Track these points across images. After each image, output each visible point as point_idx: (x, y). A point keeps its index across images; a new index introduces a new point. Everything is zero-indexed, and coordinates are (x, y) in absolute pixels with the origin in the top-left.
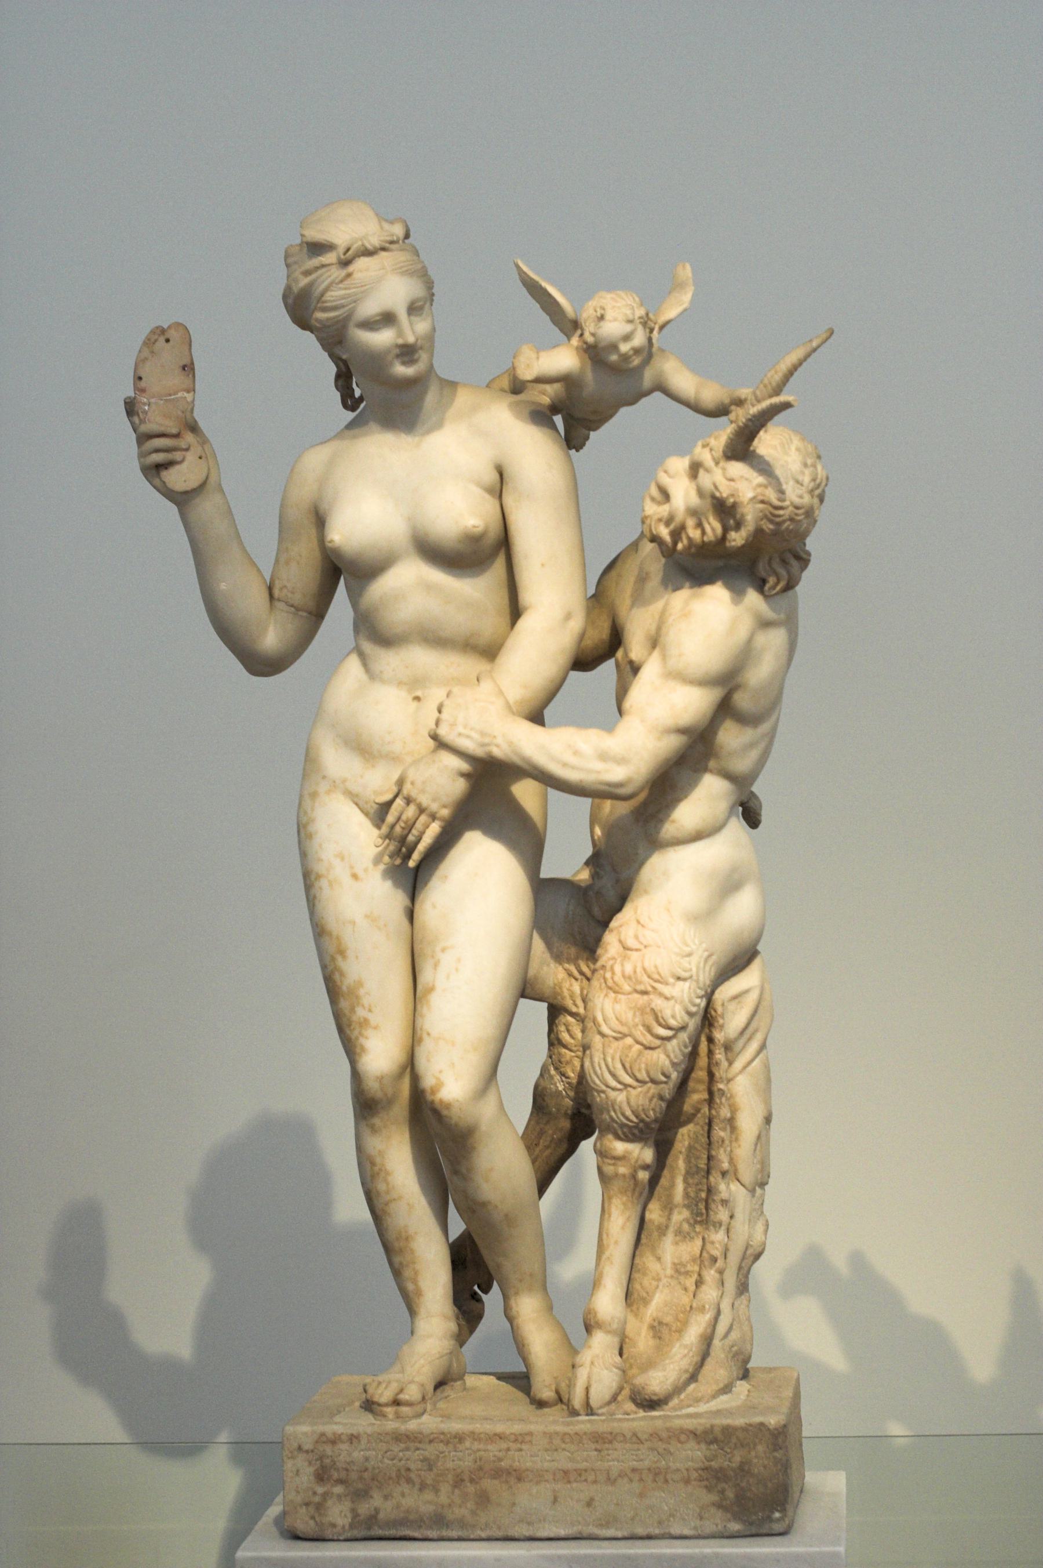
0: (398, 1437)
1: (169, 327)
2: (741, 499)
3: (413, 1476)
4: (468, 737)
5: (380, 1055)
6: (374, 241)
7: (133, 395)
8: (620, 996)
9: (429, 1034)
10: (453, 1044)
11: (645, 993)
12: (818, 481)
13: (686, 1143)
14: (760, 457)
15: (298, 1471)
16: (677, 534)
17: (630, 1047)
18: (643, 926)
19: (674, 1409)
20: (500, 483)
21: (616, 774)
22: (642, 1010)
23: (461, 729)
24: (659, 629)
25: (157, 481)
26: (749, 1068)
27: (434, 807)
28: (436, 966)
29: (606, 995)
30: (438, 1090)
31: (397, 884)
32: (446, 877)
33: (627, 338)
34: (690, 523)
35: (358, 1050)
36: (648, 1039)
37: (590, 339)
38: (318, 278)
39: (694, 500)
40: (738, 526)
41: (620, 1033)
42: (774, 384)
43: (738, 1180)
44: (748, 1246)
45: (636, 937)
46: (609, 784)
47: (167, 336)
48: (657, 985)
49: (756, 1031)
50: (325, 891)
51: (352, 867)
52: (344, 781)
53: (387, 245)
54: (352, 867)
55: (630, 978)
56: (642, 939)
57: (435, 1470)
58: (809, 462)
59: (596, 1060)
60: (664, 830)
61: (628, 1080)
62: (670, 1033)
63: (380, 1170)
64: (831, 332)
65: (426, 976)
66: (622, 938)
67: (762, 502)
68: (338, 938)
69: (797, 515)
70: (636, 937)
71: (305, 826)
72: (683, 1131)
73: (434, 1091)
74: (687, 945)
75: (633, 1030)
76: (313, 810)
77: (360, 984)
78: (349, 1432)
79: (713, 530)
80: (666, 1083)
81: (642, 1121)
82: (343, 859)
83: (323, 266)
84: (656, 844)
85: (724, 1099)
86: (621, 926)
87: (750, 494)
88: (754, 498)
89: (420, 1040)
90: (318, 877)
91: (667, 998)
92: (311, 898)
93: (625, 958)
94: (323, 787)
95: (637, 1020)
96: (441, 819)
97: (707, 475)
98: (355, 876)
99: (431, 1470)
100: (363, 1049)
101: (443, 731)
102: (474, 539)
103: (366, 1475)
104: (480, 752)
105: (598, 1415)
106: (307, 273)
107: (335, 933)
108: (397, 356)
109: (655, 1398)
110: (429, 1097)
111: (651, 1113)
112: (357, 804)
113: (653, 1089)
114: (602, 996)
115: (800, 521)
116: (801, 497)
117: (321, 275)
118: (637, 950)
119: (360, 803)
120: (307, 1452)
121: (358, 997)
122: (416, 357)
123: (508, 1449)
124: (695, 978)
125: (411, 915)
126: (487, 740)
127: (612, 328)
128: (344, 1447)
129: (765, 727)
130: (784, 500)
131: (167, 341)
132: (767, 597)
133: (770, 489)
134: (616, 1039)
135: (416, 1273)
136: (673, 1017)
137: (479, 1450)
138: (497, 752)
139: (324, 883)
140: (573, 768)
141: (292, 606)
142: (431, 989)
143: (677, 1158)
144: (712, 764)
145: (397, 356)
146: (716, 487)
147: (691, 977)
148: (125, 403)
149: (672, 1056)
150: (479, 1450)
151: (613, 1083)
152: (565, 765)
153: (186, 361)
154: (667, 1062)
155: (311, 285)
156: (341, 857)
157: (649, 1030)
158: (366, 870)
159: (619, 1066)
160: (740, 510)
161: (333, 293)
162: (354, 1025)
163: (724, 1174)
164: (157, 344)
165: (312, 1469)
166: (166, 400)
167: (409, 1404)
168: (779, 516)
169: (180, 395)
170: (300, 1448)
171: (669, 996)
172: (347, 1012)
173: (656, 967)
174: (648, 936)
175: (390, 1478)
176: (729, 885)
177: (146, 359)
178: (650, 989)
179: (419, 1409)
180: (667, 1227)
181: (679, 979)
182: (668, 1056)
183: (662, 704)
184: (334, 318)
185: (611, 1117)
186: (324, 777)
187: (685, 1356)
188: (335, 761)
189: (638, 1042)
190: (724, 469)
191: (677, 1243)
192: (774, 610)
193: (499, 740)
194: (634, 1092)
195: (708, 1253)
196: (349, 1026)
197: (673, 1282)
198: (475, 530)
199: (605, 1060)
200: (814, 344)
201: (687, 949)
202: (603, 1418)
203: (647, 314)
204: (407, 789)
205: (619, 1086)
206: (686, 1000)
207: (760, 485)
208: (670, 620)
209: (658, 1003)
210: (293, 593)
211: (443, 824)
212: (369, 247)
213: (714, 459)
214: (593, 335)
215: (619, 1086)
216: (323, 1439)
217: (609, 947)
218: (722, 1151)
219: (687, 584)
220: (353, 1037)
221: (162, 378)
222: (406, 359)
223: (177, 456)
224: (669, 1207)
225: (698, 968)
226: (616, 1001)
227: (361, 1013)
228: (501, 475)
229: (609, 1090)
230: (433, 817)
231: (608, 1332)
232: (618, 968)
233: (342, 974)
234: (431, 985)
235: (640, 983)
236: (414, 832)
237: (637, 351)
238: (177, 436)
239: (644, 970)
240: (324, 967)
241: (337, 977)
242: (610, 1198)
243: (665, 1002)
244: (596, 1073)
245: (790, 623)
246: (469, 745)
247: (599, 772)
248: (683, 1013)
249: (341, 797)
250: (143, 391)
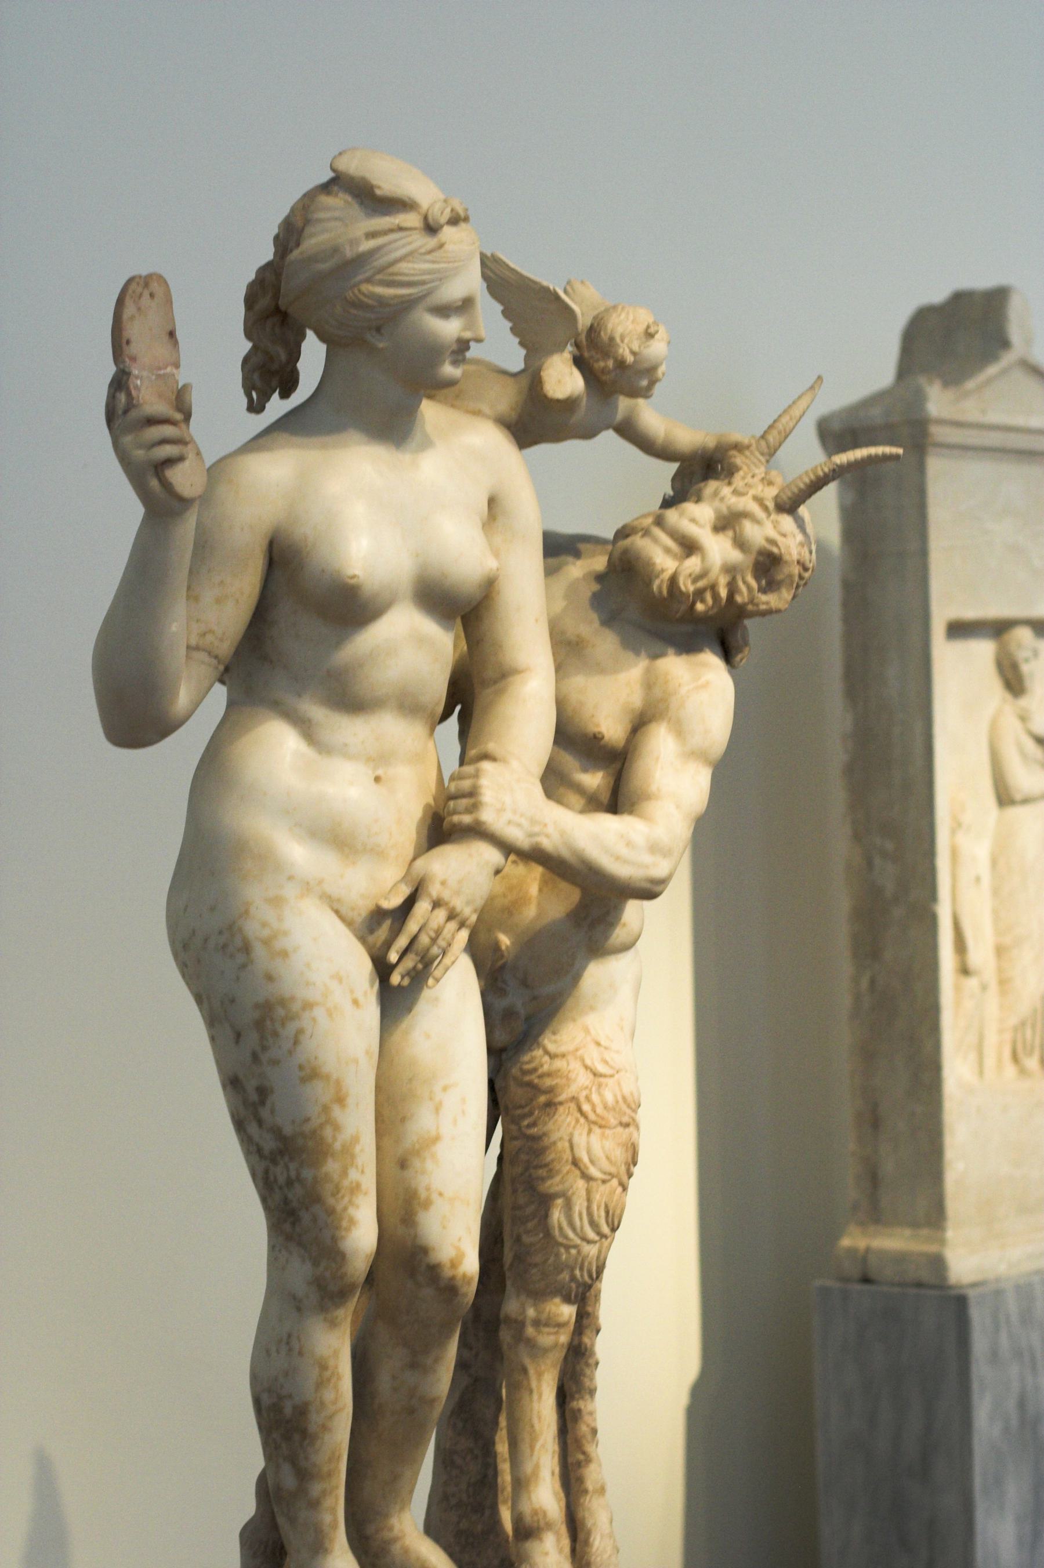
1: (150, 276)
4: (519, 825)
8: (608, 1132)
9: (441, 1194)
10: (468, 1204)
16: (699, 594)
18: (606, 1048)
23: (508, 815)
25: (154, 483)
28: (437, 1110)
29: (590, 1131)
30: (460, 1263)
32: (437, 999)
34: (723, 581)
35: (344, 1224)
37: (630, 359)
38: (390, 243)
39: (735, 556)
40: (771, 586)
41: (610, 1174)
45: (606, 1062)
51: (352, 991)
52: (321, 882)
54: (352, 991)
55: (614, 1109)
56: (611, 1062)
60: (614, 935)
63: (333, 1373)
64: (820, 378)
66: (588, 1062)
67: (798, 562)
68: (338, 1082)
70: (606, 1062)
73: (454, 1264)
76: (280, 919)
77: (355, 1139)
79: (749, 588)
82: (340, 980)
83: (401, 229)
86: (577, 1050)
89: (427, 1204)
90: (308, 1006)
93: (600, 1085)
94: (290, 891)
97: (756, 527)
98: (356, 1002)
100: (352, 1222)
101: (488, 816)
106: (372, 235)
107: (335, 1076)
110: (447, 1273)
112: (337, 912)
114: (585, 1132)
117: (395, 241)
118: (612, 1076)
119: (344, 910)
121: (353, 1157)
126: (536, 829)
131: (152, 295)
134: (604, 1182)
138: (547, 844)
139: (319, 1013)
140: (626, 862)
141: (216, 657)
142: (437, 1139)
145: (453, 352)
146: (773, 542)
151: (591, 1235)
152: (618, 858)
153: (170, 328)
155: (372, 253)
156: (339, 978)
159: (603, 1214)
160: (786, 570)
161: (410, 265)
162: (343, 1191)
166: (159, 376)
172: (336, 1177)
173: (632, 1094)
184: (403, 296)
185: (573, 1278)
186: (291, 878)
188: (298, 853)
193: (550, 830)
195: (588, 1426)
196: (333, 1195)
199: (589, 1208)
204: (435, 890)
205: (597, 1238)
208: (684, 690)
210: (221, 640)
213: (766, 509)
214: (634, 353)
217: (572, 1076)
219: (671, 651)
220: (339, 1208)
227: (353, 1175)
229: (584, 1244)
232: (595, 1097)
233: (337, 1128)
234: (433, 1133)
236: (442, 942)
239: (624, 1099)
241: (328, 1132)
242: (540, 1375)
244: (571, 1224)
246: (517, 835)
247: (647, 867)
250: (133, 359)
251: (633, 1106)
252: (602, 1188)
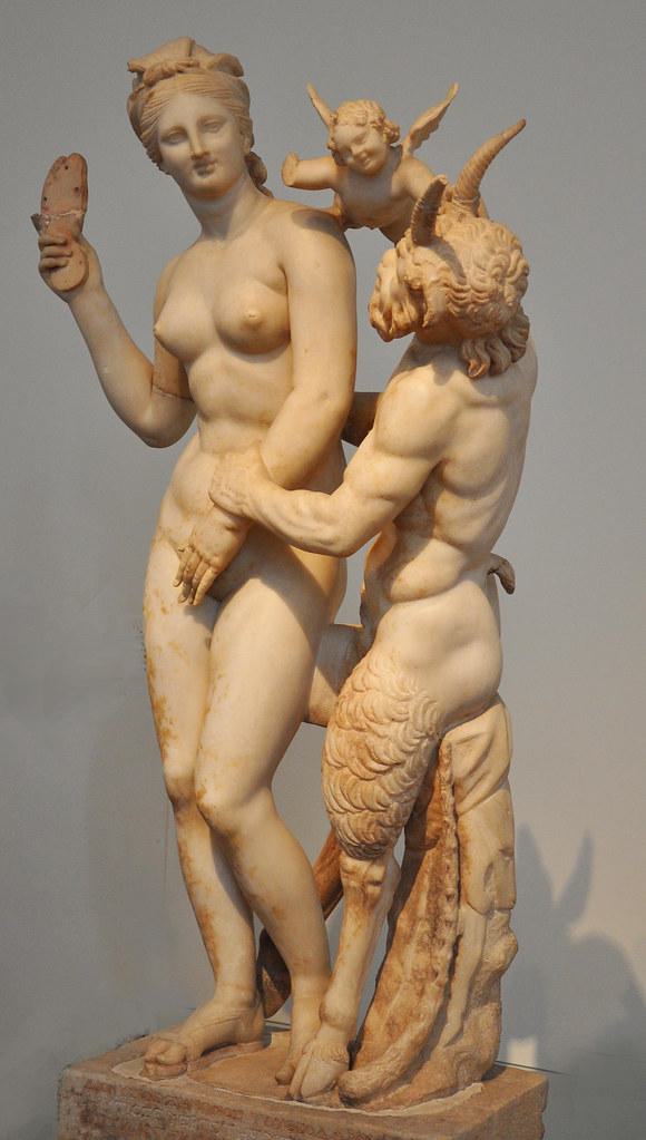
0: (145, 1095)
2: (425, 282)
3: (150, 1131)
4: (228, 496)
5: (176, 762)
6: (172, 65)
8: (343, 731)
11: (361, 730)
12: (510, 269)
13: (431, 864)
14: (447, 243)
15: (69, 1110)
17: (347, 777)
19: (373, 1109)
20: (283, 283)
21: (326, 533)
22: (358, 745)
26: (481, 806)
27: (208, 555)
31: (198, 619)
33: (359, 140)
36: (363, 771)
42: (469, 175)
43: (469, 904)
44: (480, 963)
46: (321, 541)
47: (67, 164)
48: (368, 722)
49: (487, 772)
53: (182, 68)
54: (163, 602)
55: (350, 715)
56: (366, 682)
57: (167, 1131)
58: (497, 249)
61: (348, 806)
62: (384, 768)
64: (524, 121)
67: (446, 285)
69: (478, 298)
70: (363, 679)
72: (429, 853)
73: (200, 797)
74: (403, 690)
75: (349, 761)
78: (109, 1082)
81: (363, 842)
84: (392, 601)
85: (449, 831)
87: (433, 278)
88: (438, 281)
91: (379, 736)
94: (159, 535)
95: (353, 753)
96: (217, 567)
98: (164, 610)
99: (164, 1129)
102: (254, 327)
103: (118, 1124)
104: (235, 510)
105: (307, 1103)
108: (196, 167)
109: (352, 1096)
111: (372, 836)
113: (371, 816)
115: (483, 305)
118: (362, 691)
120: (77, 1094)
122: (210, 167)
123: (223, 1123)
124: (411, 720)
125: (209, 643)
126: (239, 499)
127: (346, 132)
128: (103, 1095)
129: (488, 500)
130: (464, 284)
131: (67, 168)
132: (474, 379)
133: (452, 273)
135: (215, 946)
136: (386, 753)
137: (202, 1119)
140: (295, 525)
143: (423, 876)
144: (436, 531)
145: (196, 167)
147: (407, 719)
148: (32, 218)
149: (387, 787)
150: (202, 1119)
151: (336, 807)
152: (290, 523)
153: (78, 184)
154: (383, 793)
157: (363, 762)
163: (449, 897)
164: (60, 171)
165: (78, 1111)
167: (166, 1065)
168: (462, 299)
169: (72, 212)
170: (73, 1090)
171: (381, 734)
173: (372, 707)
174: (372, 680)
175: (134, 1129)
176: (453, 639)
177: (50, 184)
178: (364, 726)
179: (174, 1069)
180: (411, 936)
181: (393, 720)
182: (384, 788)
183: (375, 470)
187: (393, 1059)
188: (170, 517)
189: (354, 773)
190: (413, 254)
191: (418, 952)
192: (483, 393)
193: (248, 500)
194: (353, 817)
197: (412, 986)
200: (505, 136)
201: (404, 694)
202: (310, 1106)
203: (382, 120)
205: (342, 811)
206: (400, 739)
207: (442, 269)
209: (372, 740)
211: (215, 570)
212: (166, 69)
215: (342, 811)
216: (89, 1085)
218: (447, 876)
221: (65, 202)
222: (202, 169)
223: (62, 261)
224: (414, 920)
225: (415, 712)
226: (339, 735)
228: (284, 271)
230: (208, 563)
231: (333, 1026)
235: (357, 720)
237: (371, 154)
238: (65, 244)
239: (363, 709)
243: (379, 740)
245: (517, 410)
247: (314, 531)
248: (397, 751)
249: (167, 543)
251: (371, 716)
252: (336, 772)
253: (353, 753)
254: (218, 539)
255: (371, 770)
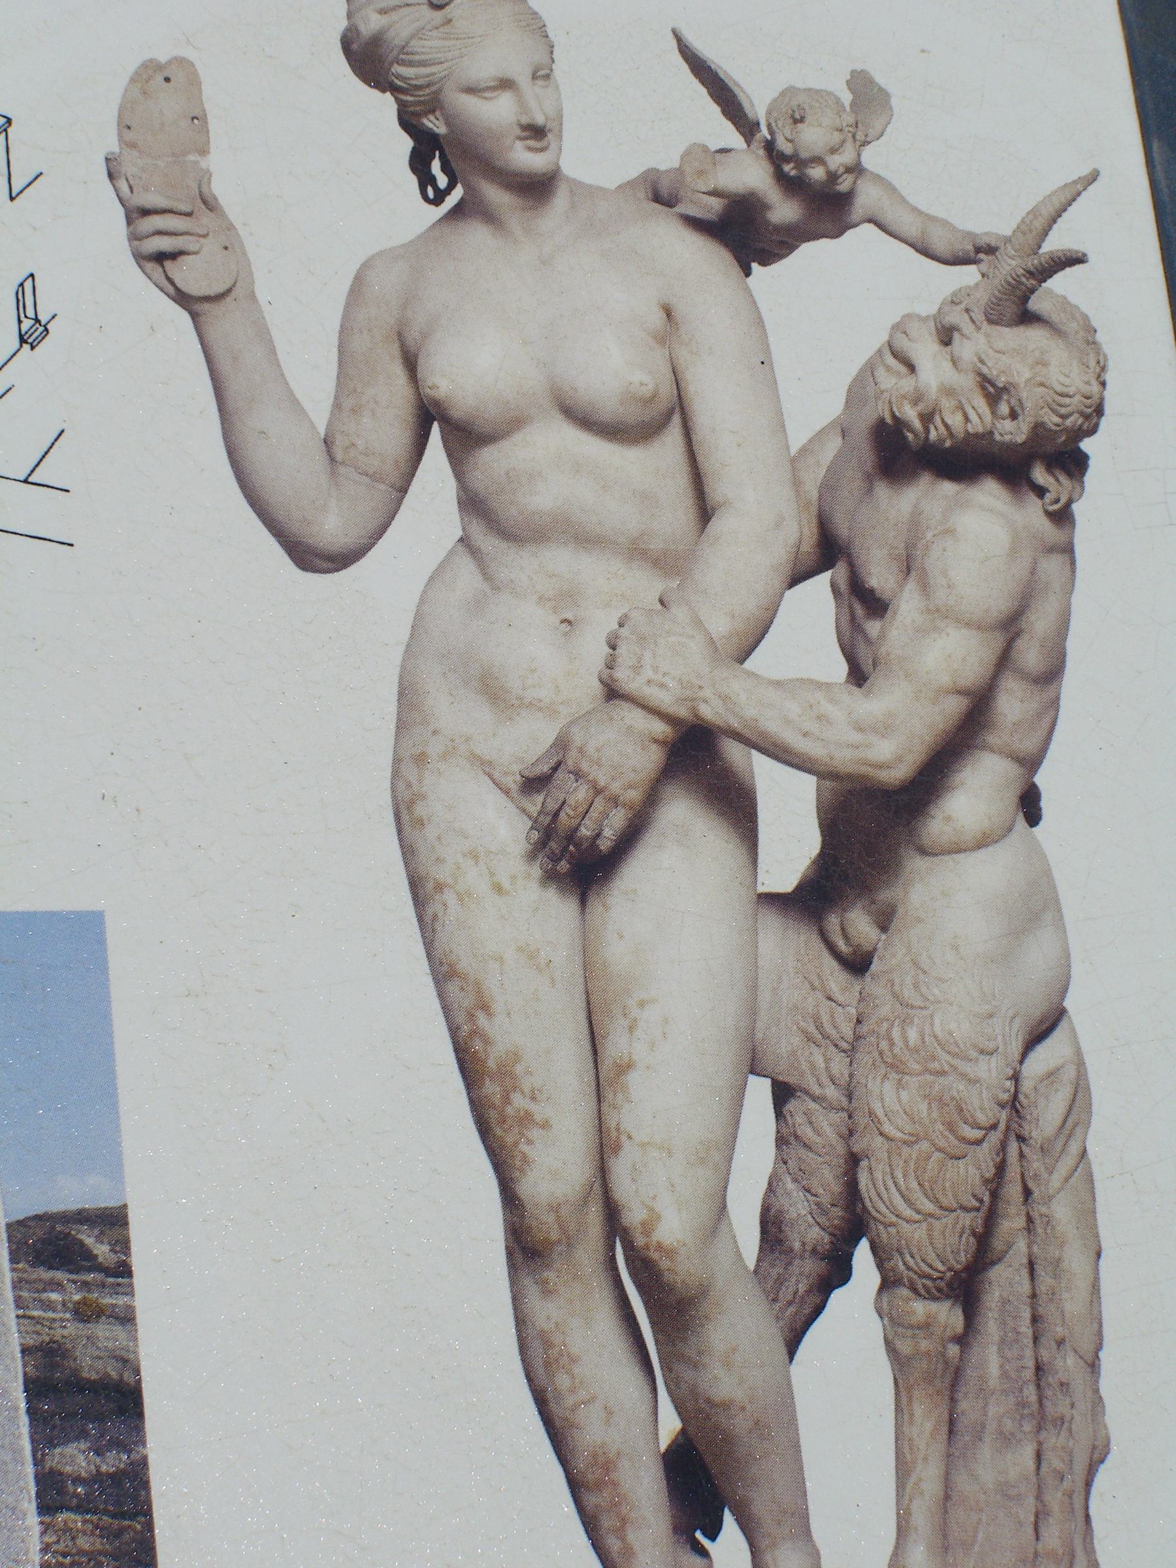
7: (117, 150)
11: (942, 1073)
24: (910, 547)
50: (449, 907)
51: (492, 874)
55: (917, 1051)
59: (878, 1175)
61: (929, 1207)
65: (616, 1045)
71: (410, 805)
80: (978, 1209)
92: (428, 919)
116: (1088, 383)
139: (449, 897)
151: (908, 1212)
156: (474, 856)
157: (951, 1127)
158: (513, 878)
178: (946, 1068)
198: (644, 388)
205: (918, 1217)
208: (929, 535)
209: (959, 1088)
215: (918, 1217)
229: (900, 1221)
240: (454, 1031)
253: (935, 1115)
254: (625, 751)
255: (963, 1140)
